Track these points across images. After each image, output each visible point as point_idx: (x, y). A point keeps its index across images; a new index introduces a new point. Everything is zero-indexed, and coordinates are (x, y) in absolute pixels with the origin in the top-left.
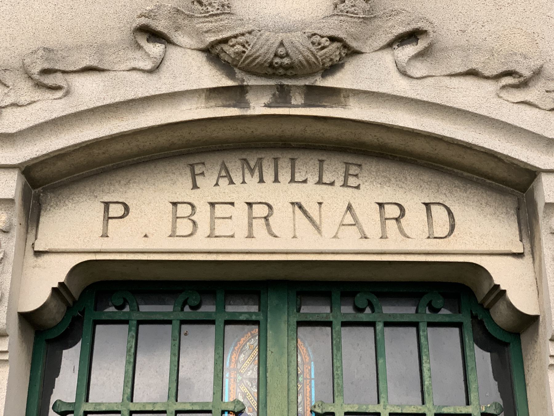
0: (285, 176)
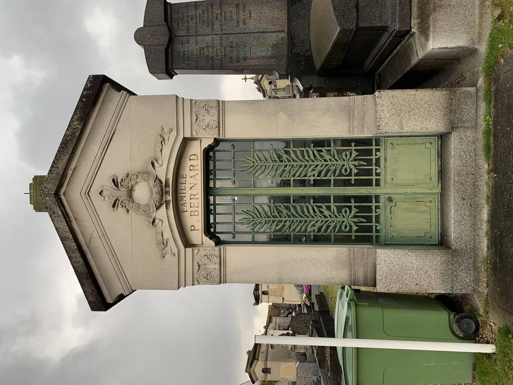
0: (184, 191)
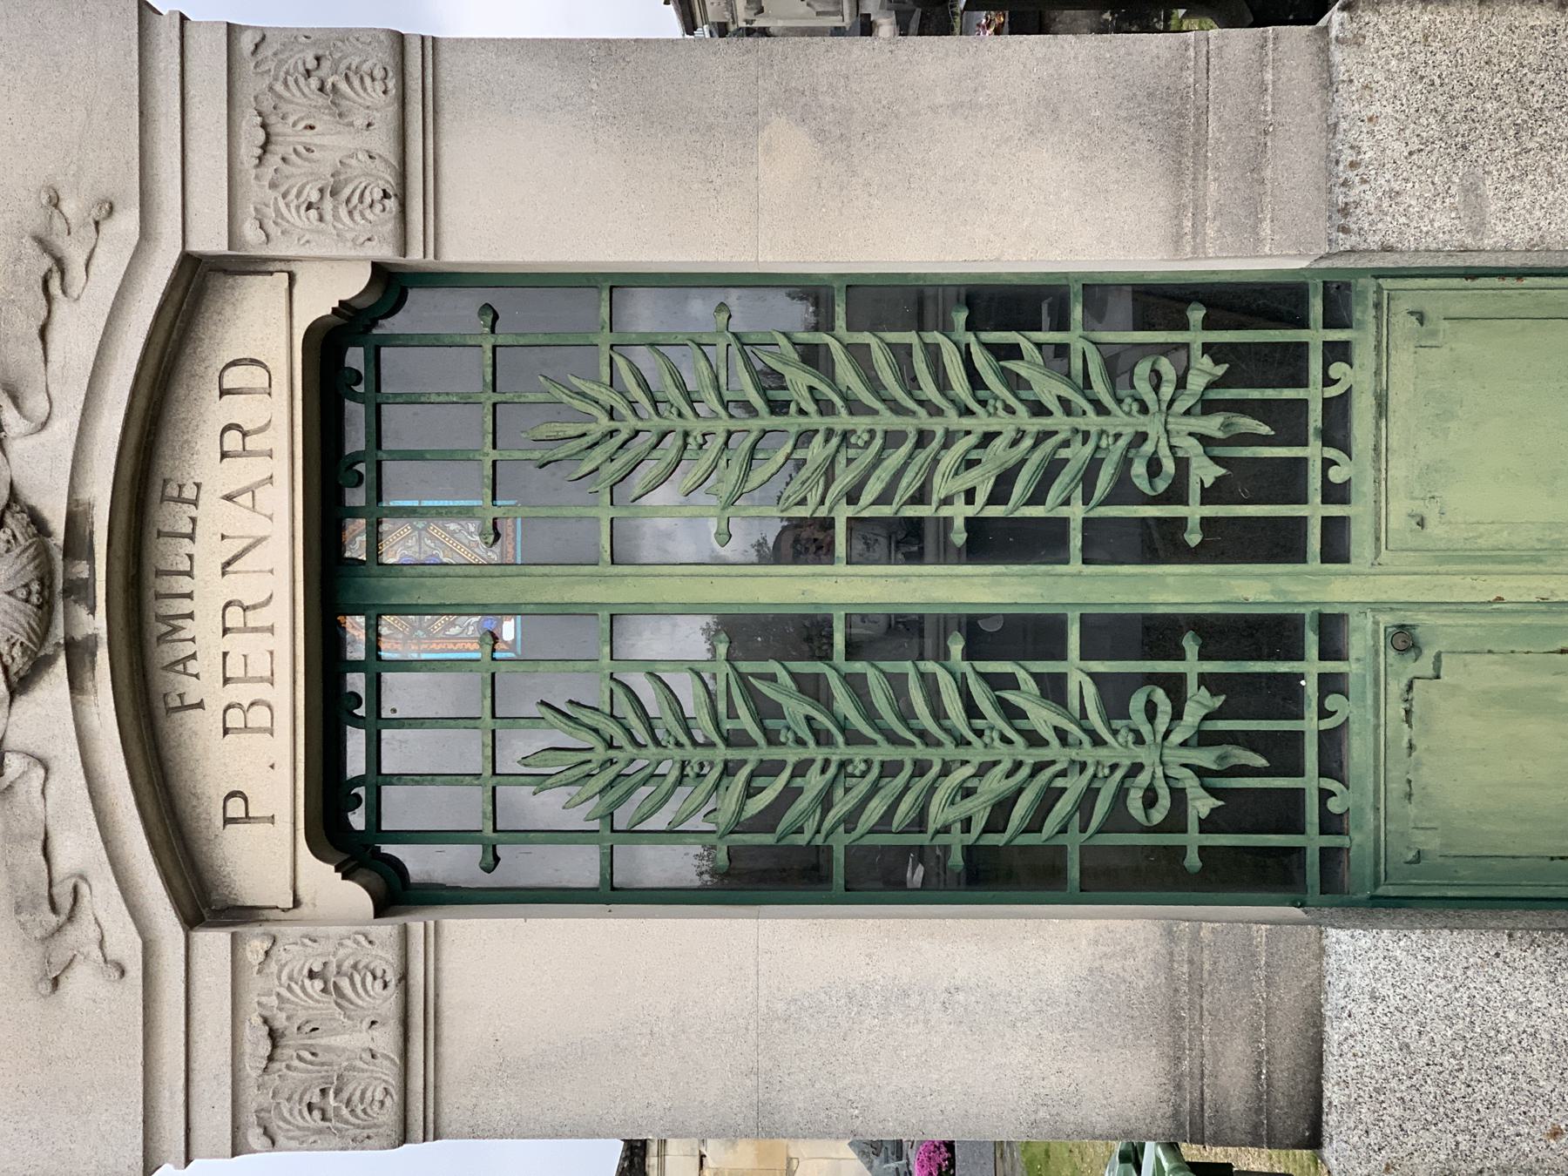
0: (183, 585)
